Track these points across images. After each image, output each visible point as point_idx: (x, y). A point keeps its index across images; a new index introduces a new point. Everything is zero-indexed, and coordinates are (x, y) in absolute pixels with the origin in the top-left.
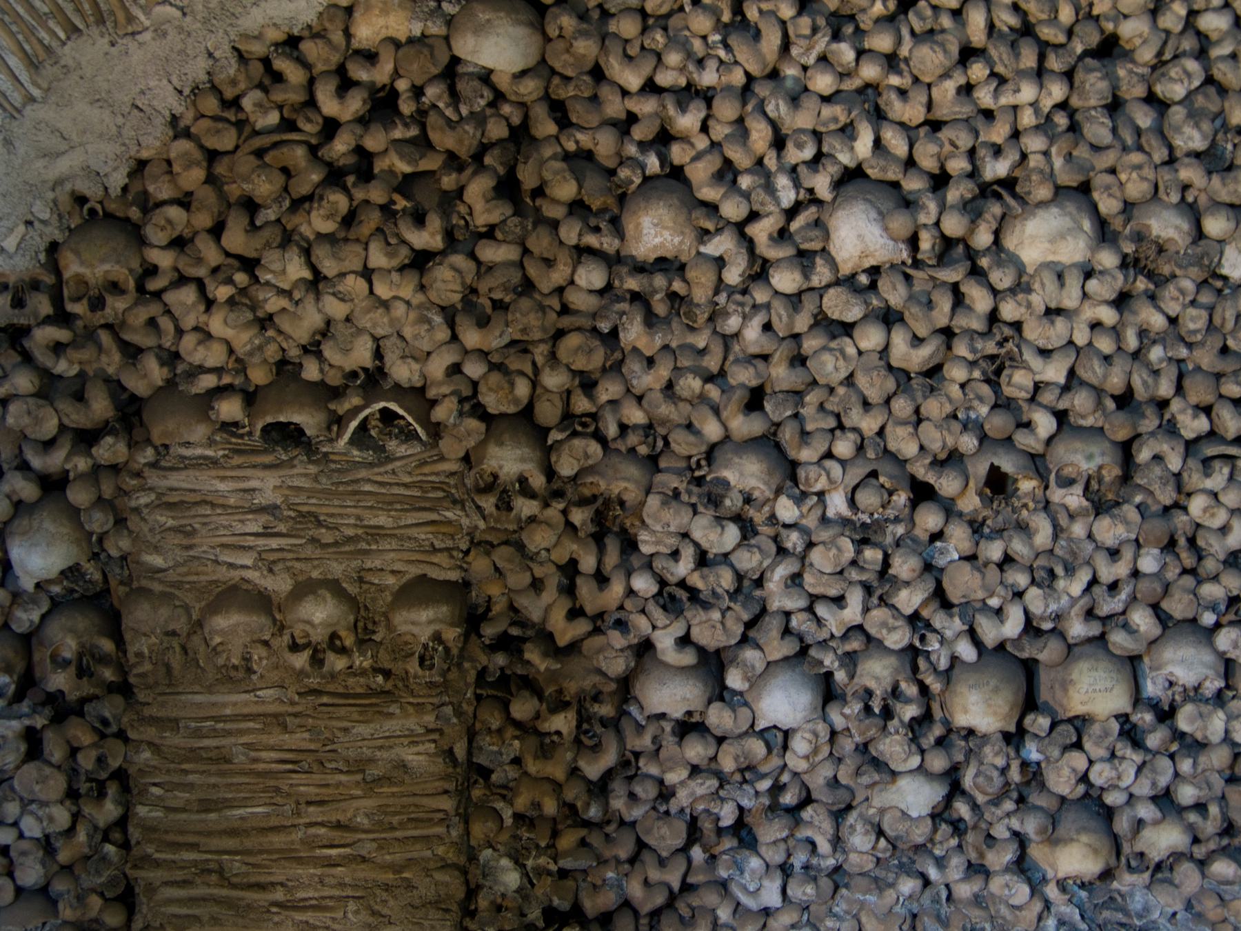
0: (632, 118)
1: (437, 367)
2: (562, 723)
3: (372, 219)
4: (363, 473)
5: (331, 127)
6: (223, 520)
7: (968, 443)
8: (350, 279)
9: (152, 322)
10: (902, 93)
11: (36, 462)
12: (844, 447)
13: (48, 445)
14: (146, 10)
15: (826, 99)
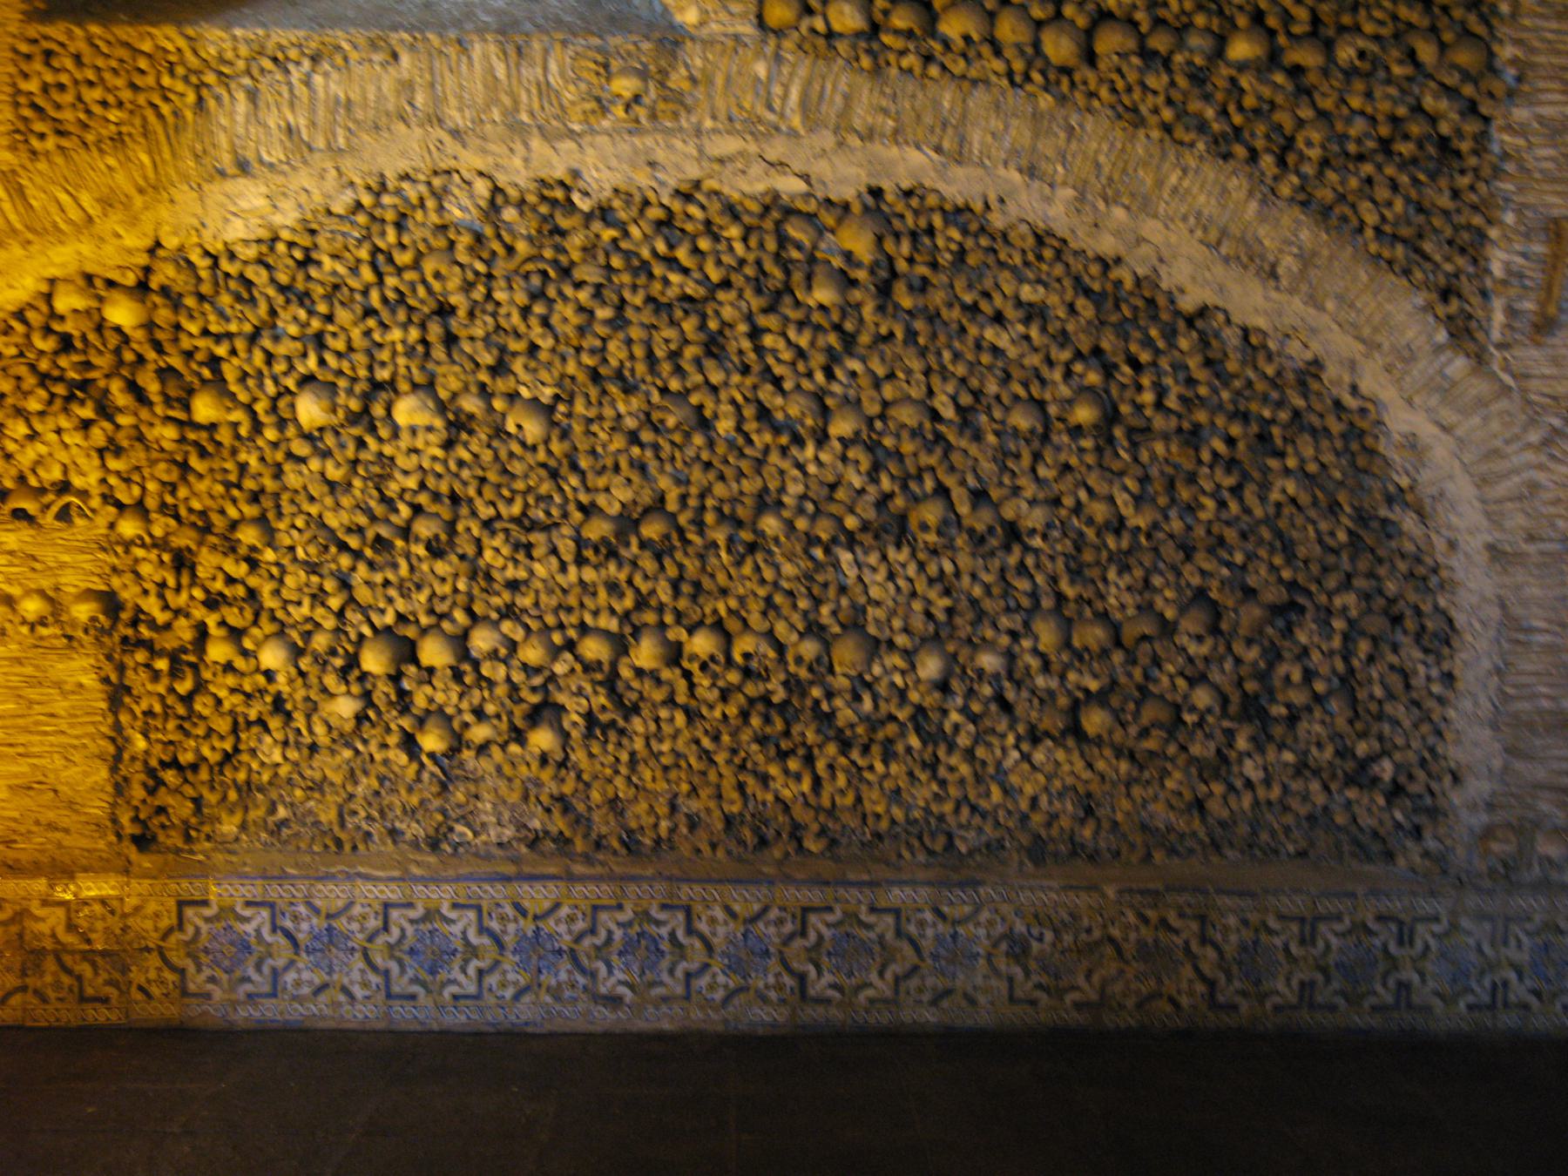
3: (58, 403)
5: (42, 352)
7: (362, 520)
10: (334, 335)
12: (300, 523)
15: (294, 338)
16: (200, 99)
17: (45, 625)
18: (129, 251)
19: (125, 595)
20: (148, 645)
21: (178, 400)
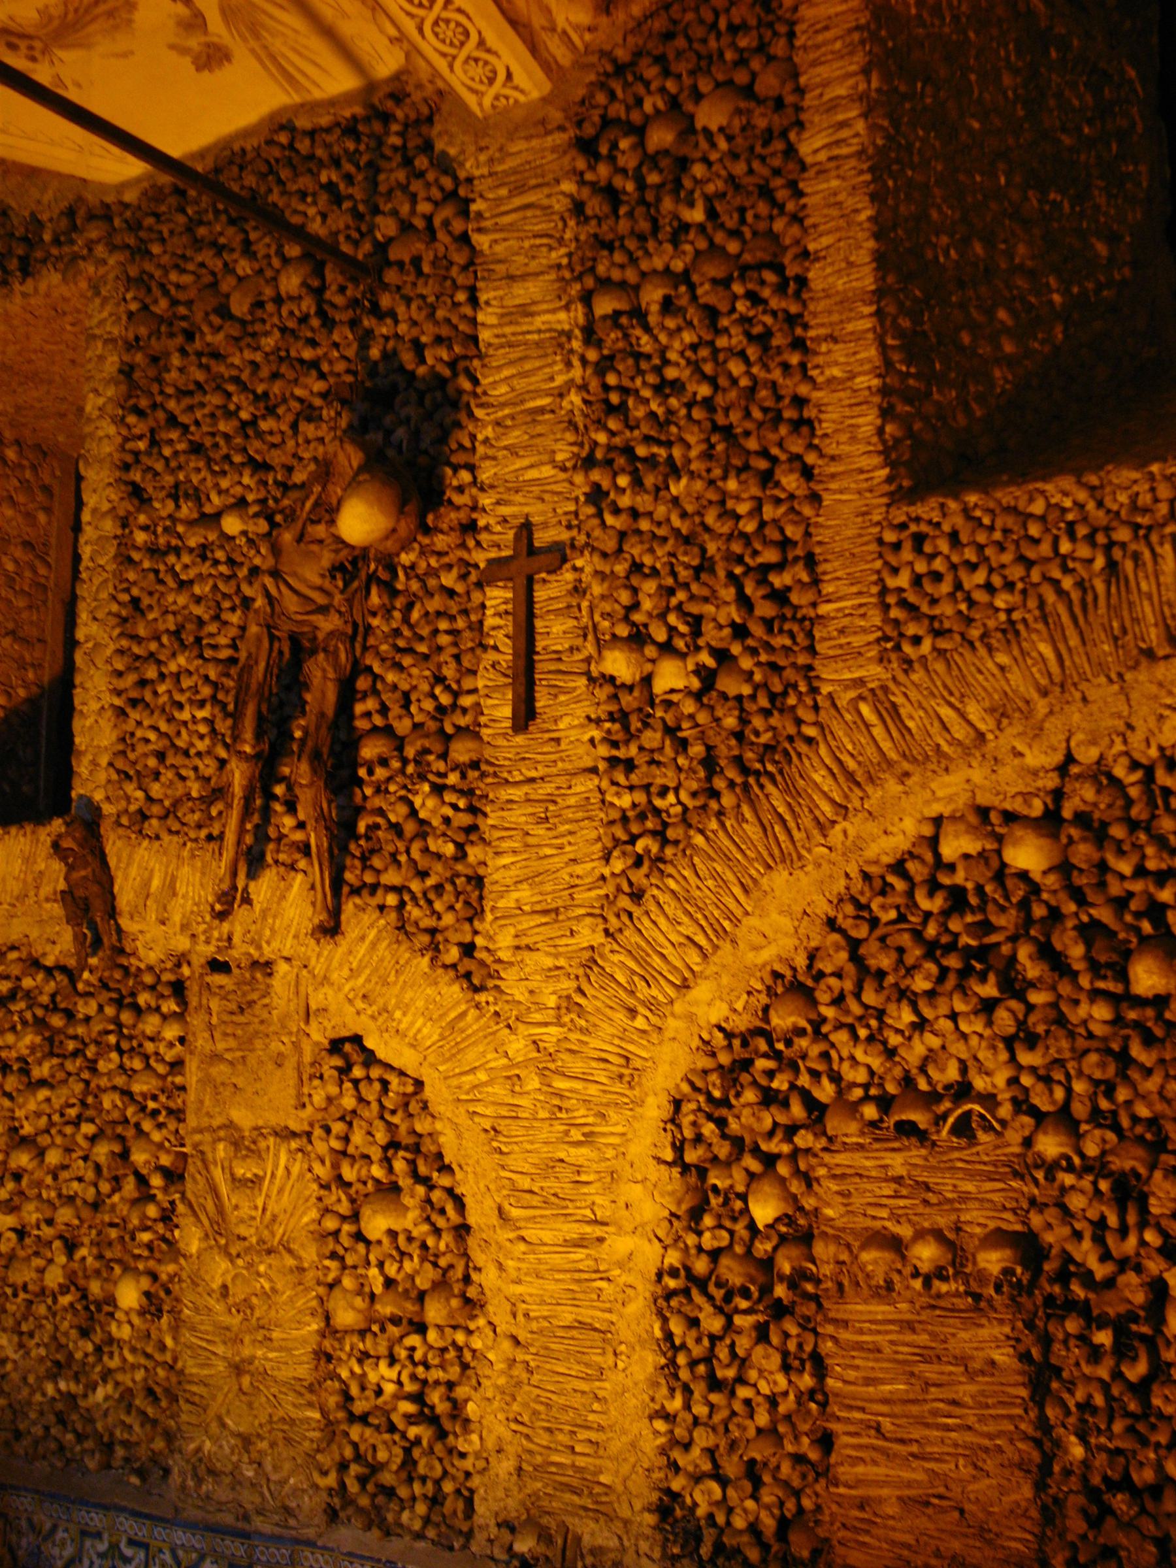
0: (1131, 895)
1: (1000, 1079)
2: (1103, 1338)
3: (951, 981)
4: (956, 1155)
5: (928, 915)
6: (868, 1186)
8: (942, 1021)
9: (825, 1056)
11: (764, 1147)
13: (771, 1134)
14: (809, 851)
16: (1112, 566)
17: (945, 1279)
18: (1035, 773)
19: (1049, 1238)
20: (1084, 1310)
21: (1109, 965)
